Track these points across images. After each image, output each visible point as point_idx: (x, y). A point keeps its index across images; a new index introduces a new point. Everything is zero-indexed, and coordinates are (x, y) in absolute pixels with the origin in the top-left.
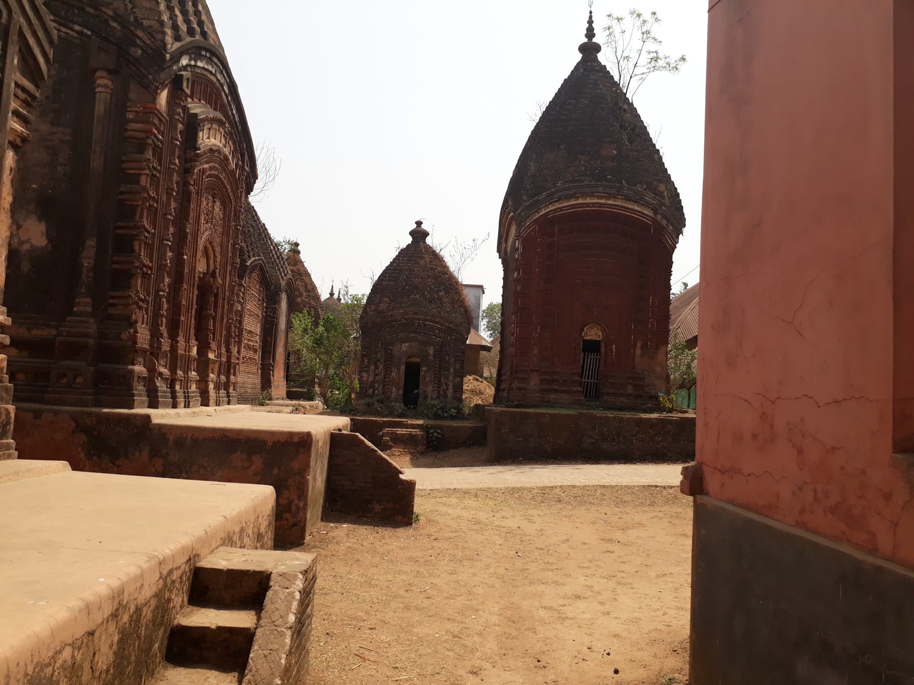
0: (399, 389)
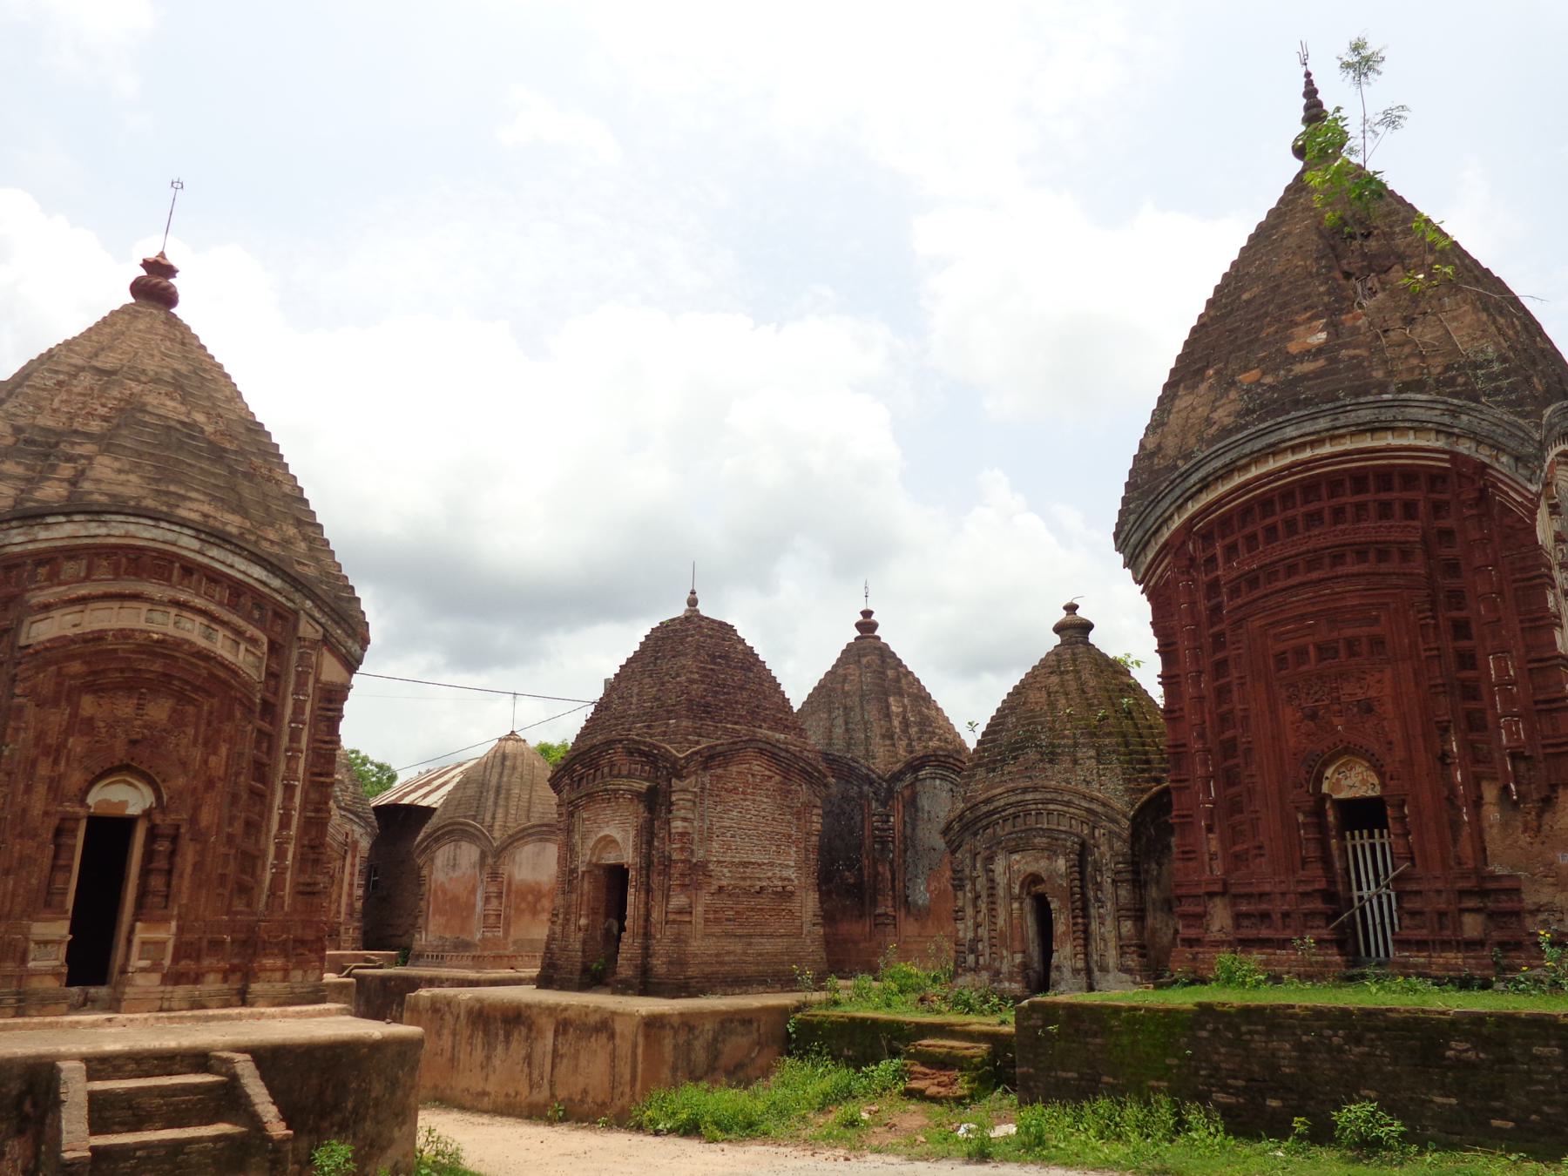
0: (1015, 952)
